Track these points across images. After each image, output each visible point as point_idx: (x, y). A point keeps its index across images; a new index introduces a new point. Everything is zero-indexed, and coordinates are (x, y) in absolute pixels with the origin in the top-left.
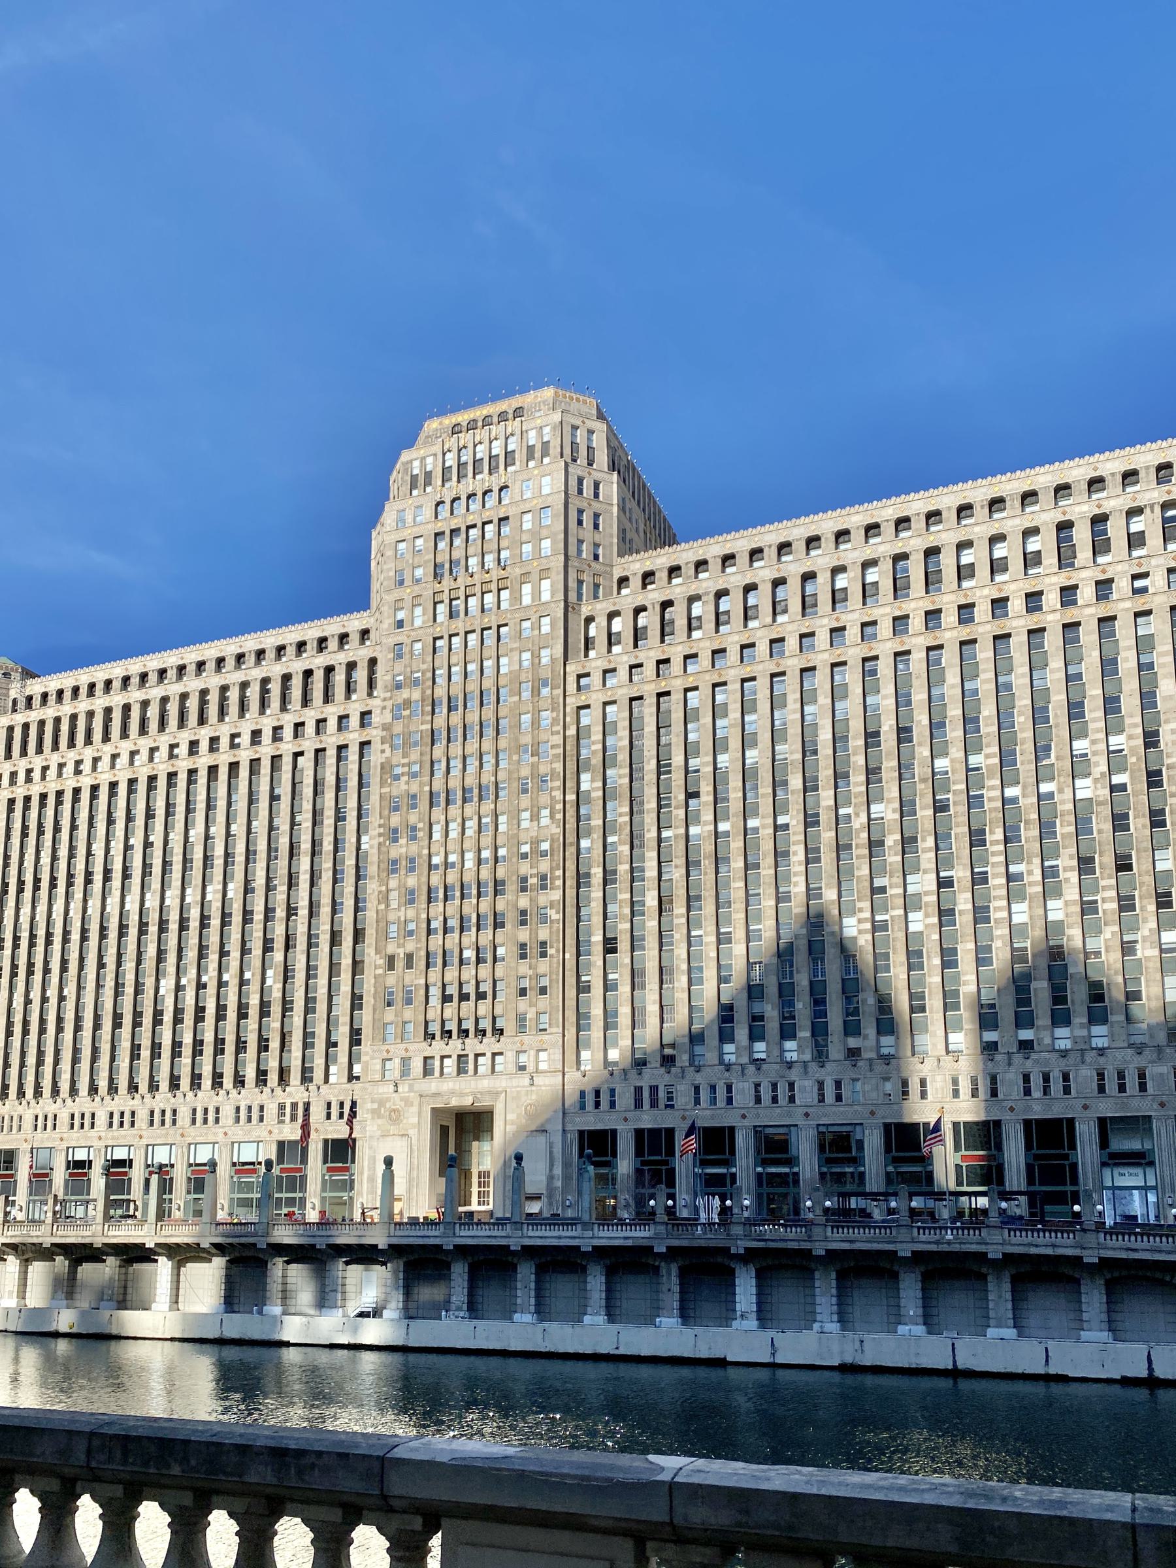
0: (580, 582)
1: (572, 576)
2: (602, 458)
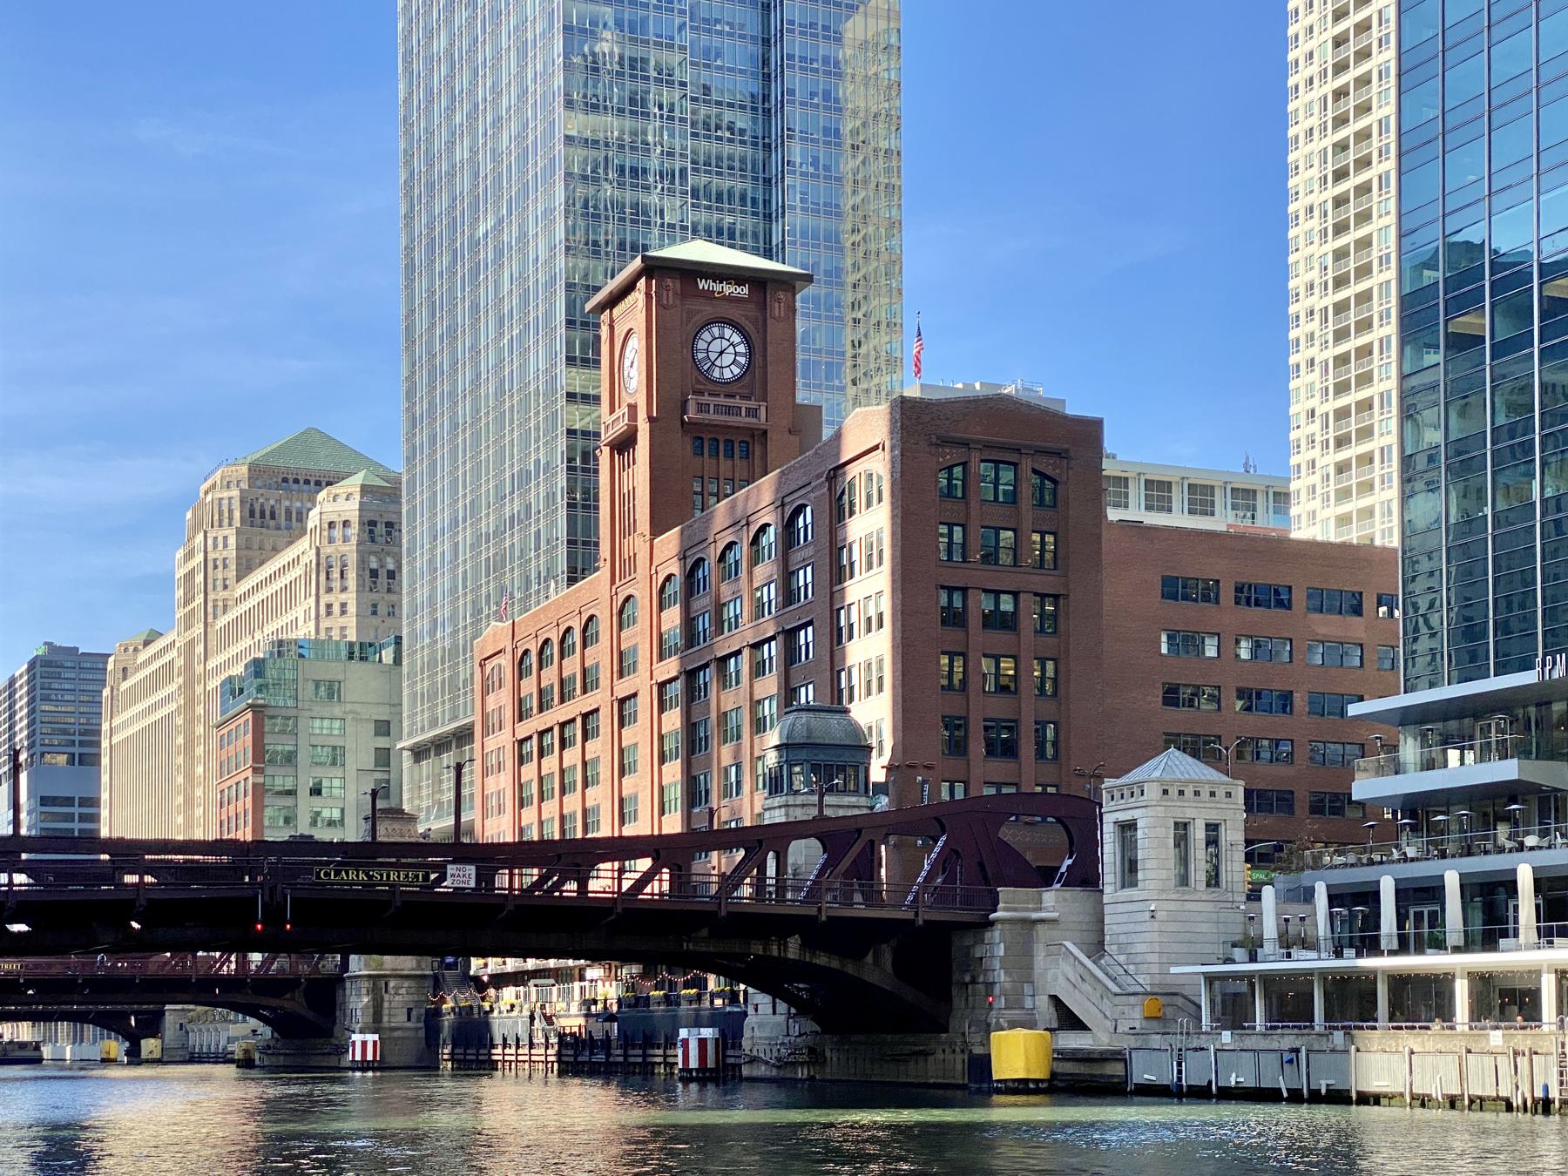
1: (210, 604)
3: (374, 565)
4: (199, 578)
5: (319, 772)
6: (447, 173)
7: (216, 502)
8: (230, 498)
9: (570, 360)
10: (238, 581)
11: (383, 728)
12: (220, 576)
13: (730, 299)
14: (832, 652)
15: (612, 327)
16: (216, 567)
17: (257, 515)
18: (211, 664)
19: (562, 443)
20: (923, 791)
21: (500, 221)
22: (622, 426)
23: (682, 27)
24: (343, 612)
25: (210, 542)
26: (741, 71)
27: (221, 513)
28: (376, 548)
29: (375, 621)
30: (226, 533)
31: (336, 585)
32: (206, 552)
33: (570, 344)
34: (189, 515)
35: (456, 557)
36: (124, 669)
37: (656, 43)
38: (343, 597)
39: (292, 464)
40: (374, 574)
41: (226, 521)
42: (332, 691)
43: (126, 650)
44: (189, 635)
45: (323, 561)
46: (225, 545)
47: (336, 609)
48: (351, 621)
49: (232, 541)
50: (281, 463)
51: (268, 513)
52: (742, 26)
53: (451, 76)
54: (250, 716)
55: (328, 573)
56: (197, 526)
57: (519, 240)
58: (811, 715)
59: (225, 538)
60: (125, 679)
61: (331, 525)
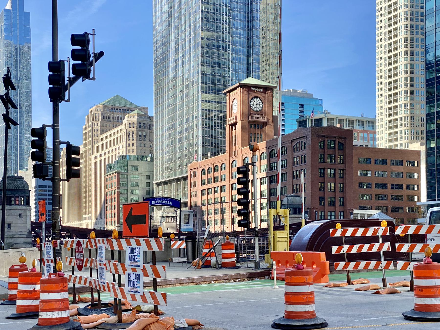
0: (95, 141)
2: (100, 118)
3: (140, 134)
4: (90, 134)
5: (132, 188)
6: (167, 42)
7: (95, 114)
8: (98, 114)
9: (203, 92)
11: (148, 177)
12: (96, 133)
13: (259, 92)
14: (292, 181)
15: (230, 97)
16: (95, 131)
18: (94, 156)
19: (200, 112)
20: (316, 214)
21: (183, 56)
22: (234, 121)
23: (229, 10)
24: (133, 146)
25: (93, 125)
26: (242, 20)
28: (141, 129)
29: (141, 148)
30: (97, 122)
31: (131, 139)
32: (92, 127)
33: (202, 88)
34: (86, 117)
35: (170, 137)
37: (223, 14)
38: (133, 142)
41: (97, 119)
42: (135, 168)
44: (87, 148)
46: (97, 126)
47: (131, 145)
48: (135, 148)
49: (99, 124)
50: (111, 104)
52: (242, 9)
53: (168, 18)
54: (116, 174)
56: (89, 120)
57: (188, 61)
58: (292, 197)
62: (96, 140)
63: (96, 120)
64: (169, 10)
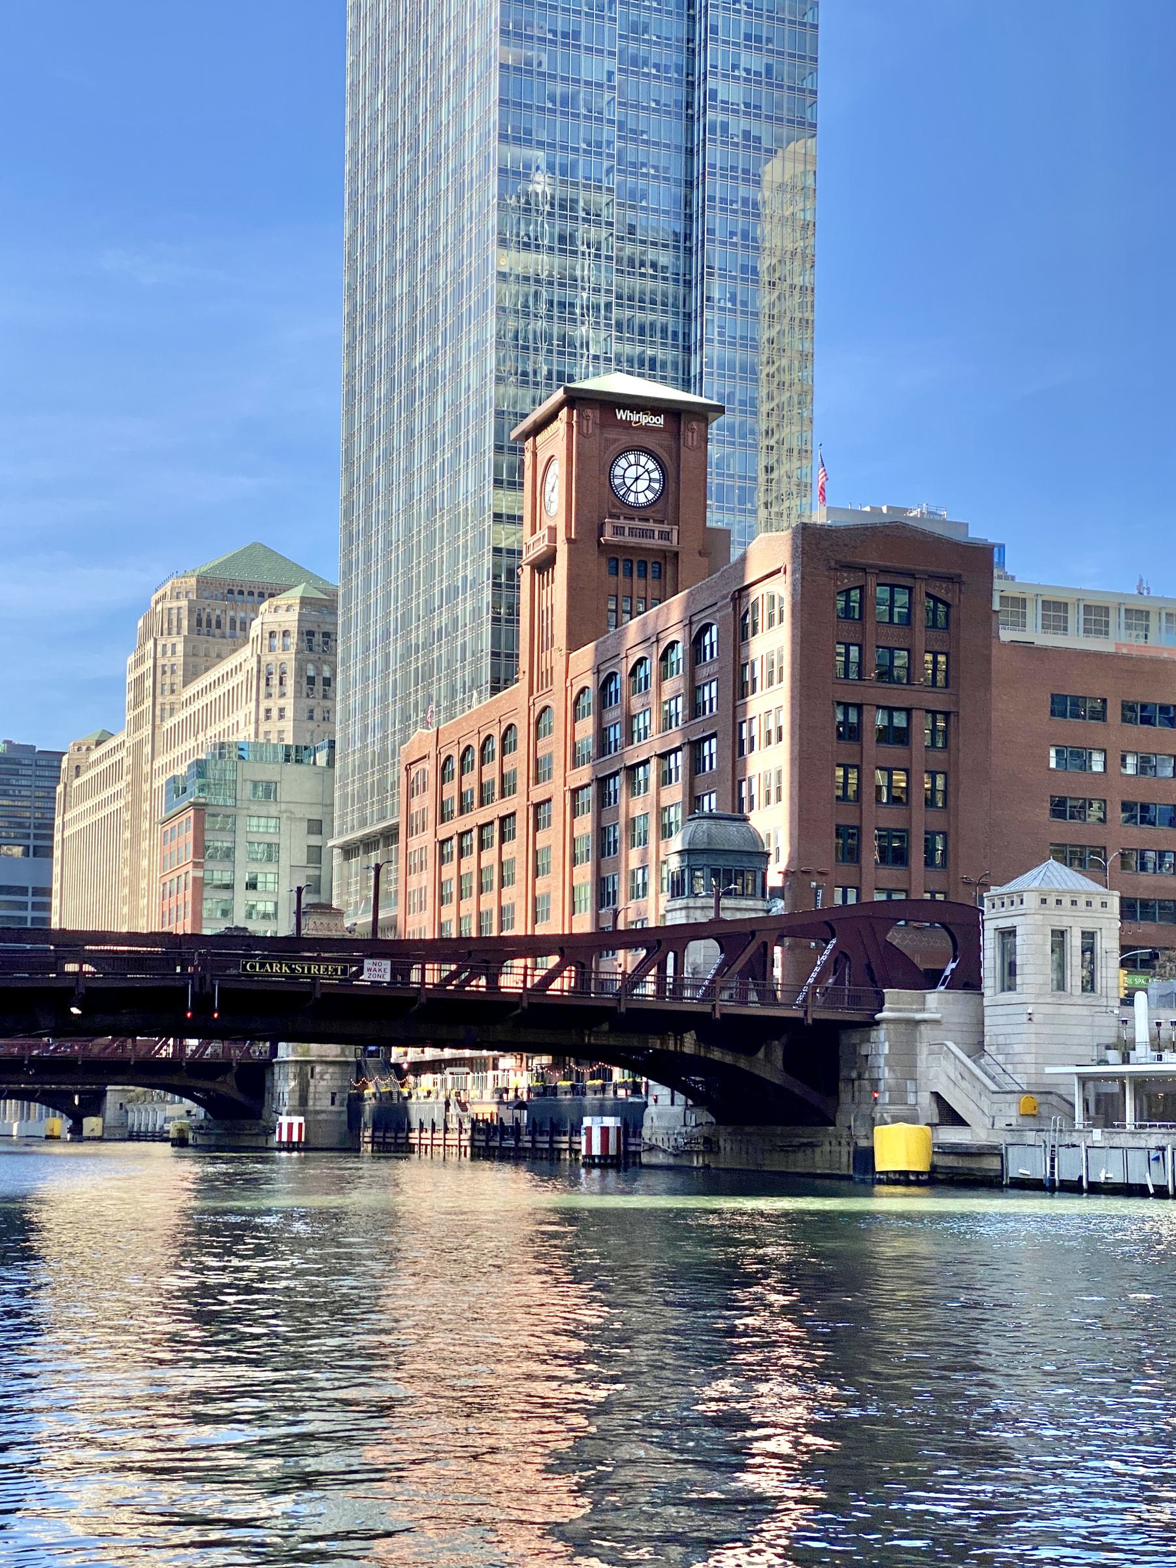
1: (158, 708)
3: (311, 673)
4: (149, 683)
5: (255, 868)
6: (387, 306)
7: (166, 612)
8: (179, 608)
9: (498, 483)
10: (184, 686)
11: (316, 827)
12: (168, 681)
13: (646, 429)
14: (734, 762)
15: (535, 455)
16: (164, 672)
17: (204, 624)
18: (159, 762)
19: (488, 561)
20: (816, 895)
21: (435, 351)
22: (541, 548)
23: (610, 170)
24: (281, 717)
25: (159, 648)
26: (664, 212)
27: (170, 622)
28: (312, 656)
29: (311, 725)
30: (174, 640)
31: (275, 690)
32: (155, 659)
33: (498, 468)
34: (140, 623)
35: (387, 667)
36: (78, 767)
37: (585, 186)
38: (282, 702)
39: (237, 576)
40: (311, 681)
41: (175, 630)
42: (269, 791)
43: (79, 749)
44: (138, 736)
45: (263, 668)
46: (174, 652)
47: (275, 714)
48: (288, 725)
49: (180, 648)
50: (226, 576)
51: (214, 622)
52: (666, 170)
53: (393, 215)
54: (192, 813)
55: (268, 679)
56: (148, 633)
57: (452, 369)
58: (712, 822)
59: (174, 645)
60: (77, 776)
61: (272, 634)
62: (168, 707)
63: (169, 634)
64: (395, 185)
